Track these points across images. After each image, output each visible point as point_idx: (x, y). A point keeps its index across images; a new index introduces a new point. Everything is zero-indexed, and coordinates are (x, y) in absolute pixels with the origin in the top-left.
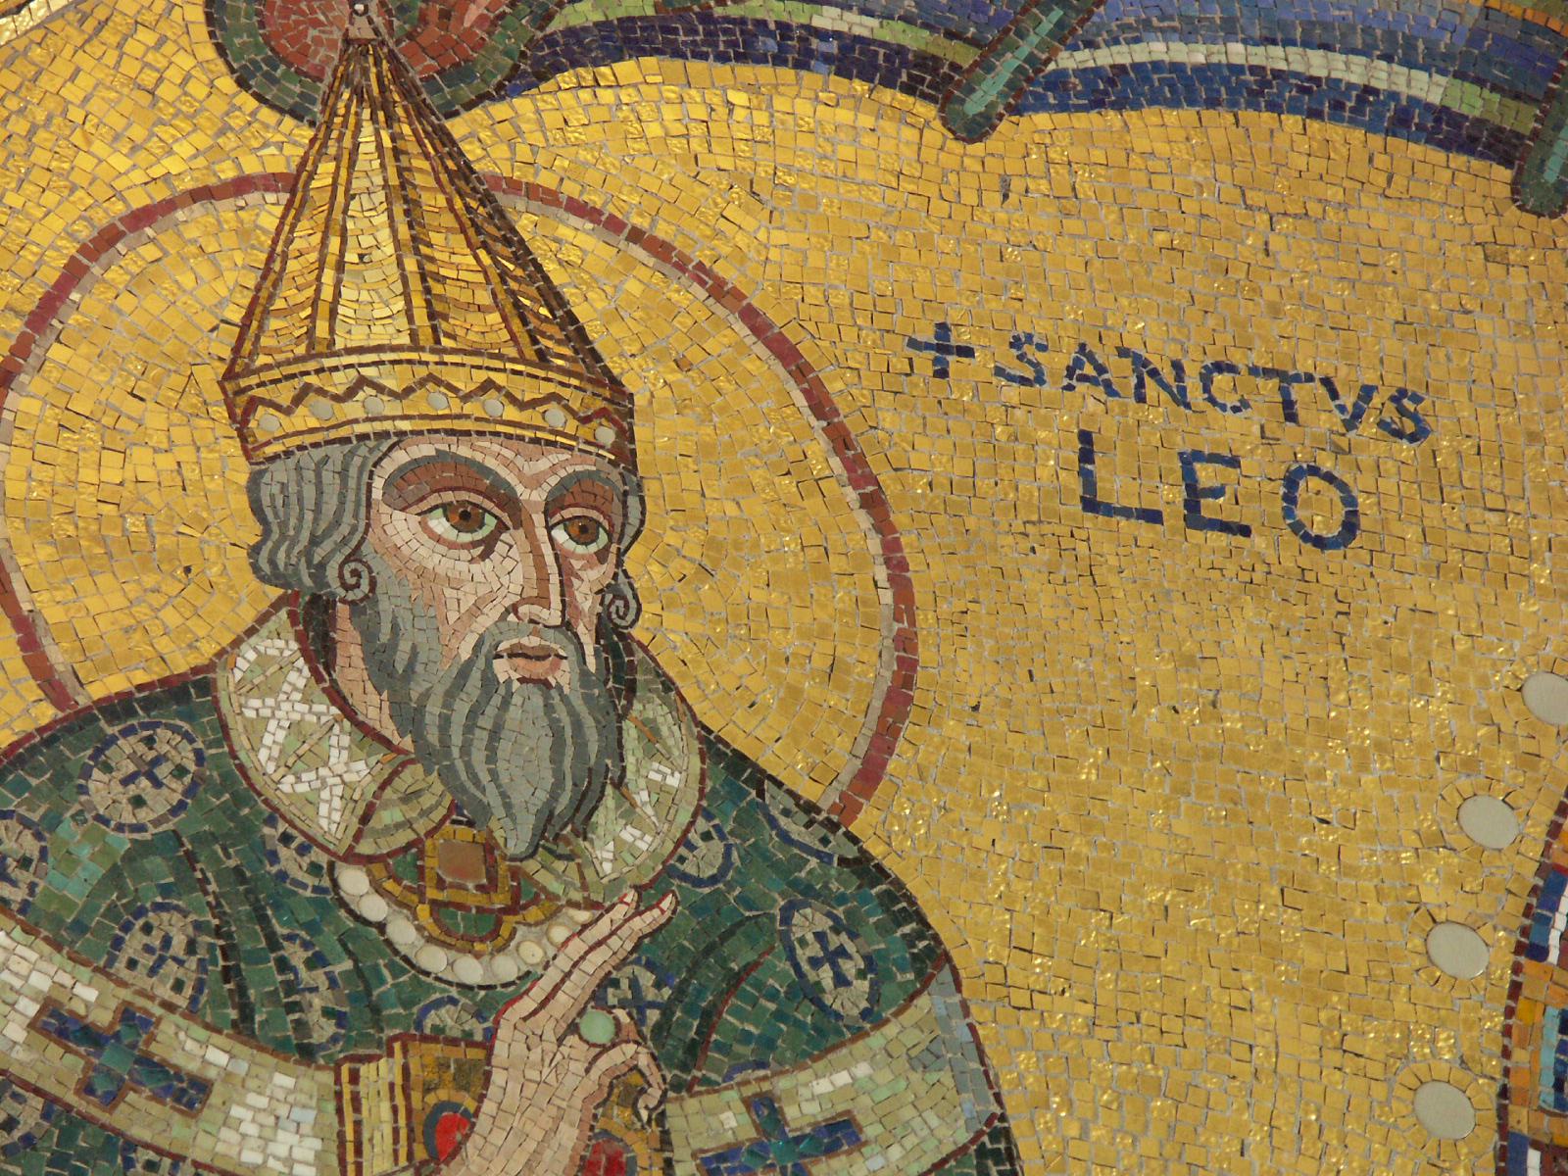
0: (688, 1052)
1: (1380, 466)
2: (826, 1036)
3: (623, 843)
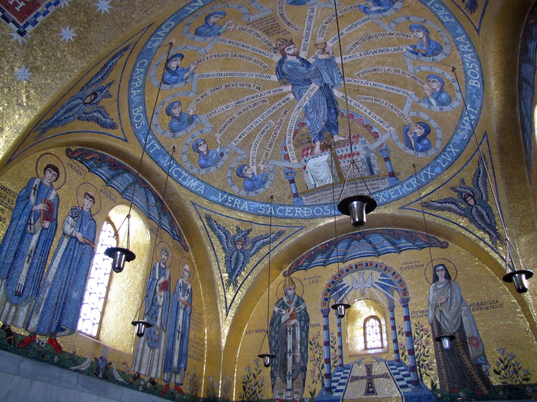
0: (296, 306)
1: (319, 279)
2: (300, 305)
3: (295, 300)
